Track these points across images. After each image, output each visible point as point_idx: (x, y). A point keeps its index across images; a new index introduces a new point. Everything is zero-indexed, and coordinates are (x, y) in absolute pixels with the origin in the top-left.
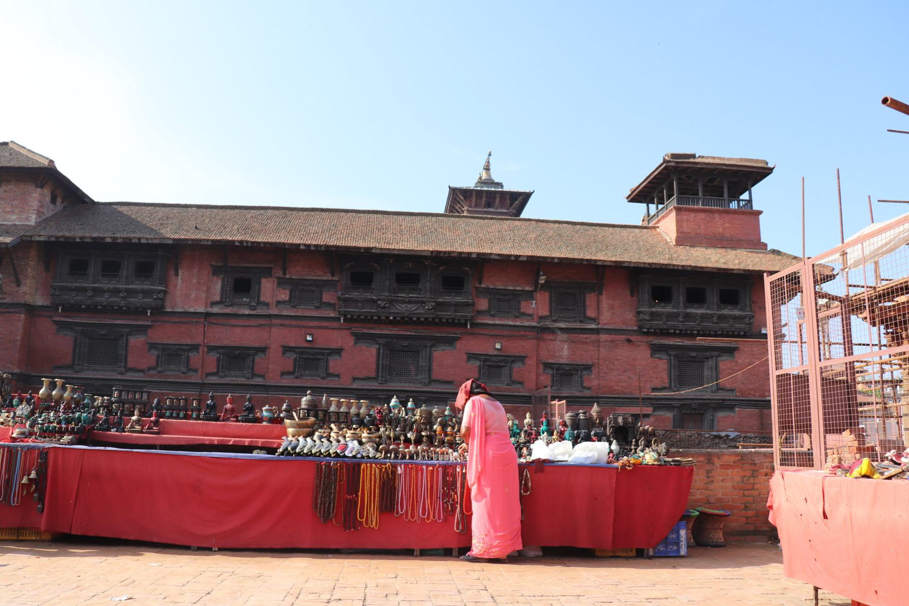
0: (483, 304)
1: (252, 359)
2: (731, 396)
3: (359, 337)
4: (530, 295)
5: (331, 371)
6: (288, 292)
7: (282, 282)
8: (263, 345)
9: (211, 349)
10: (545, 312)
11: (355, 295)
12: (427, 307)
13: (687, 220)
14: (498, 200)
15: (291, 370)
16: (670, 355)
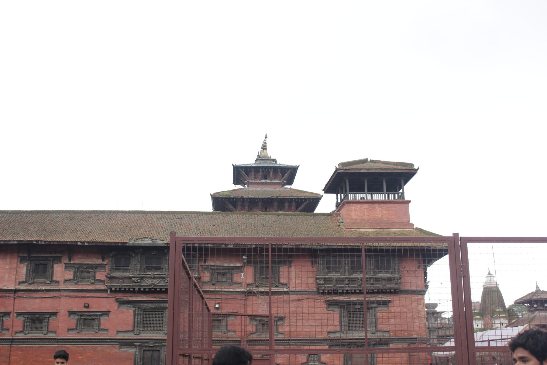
0: (206, 276)
1: (47, 320)
2: (386, 335)
3: (121, 303)
4: (240, 269)
5: (101, 327)
6: (72, 273)
7: (67, 266)
8: (54, 311)
9: (19, 314)
10: (250, 280)
11: (117, 274)
12: (166, 281)
13: (355, 210)
14: (271, 173)
15: (75, 327)
16: (341, 308)
